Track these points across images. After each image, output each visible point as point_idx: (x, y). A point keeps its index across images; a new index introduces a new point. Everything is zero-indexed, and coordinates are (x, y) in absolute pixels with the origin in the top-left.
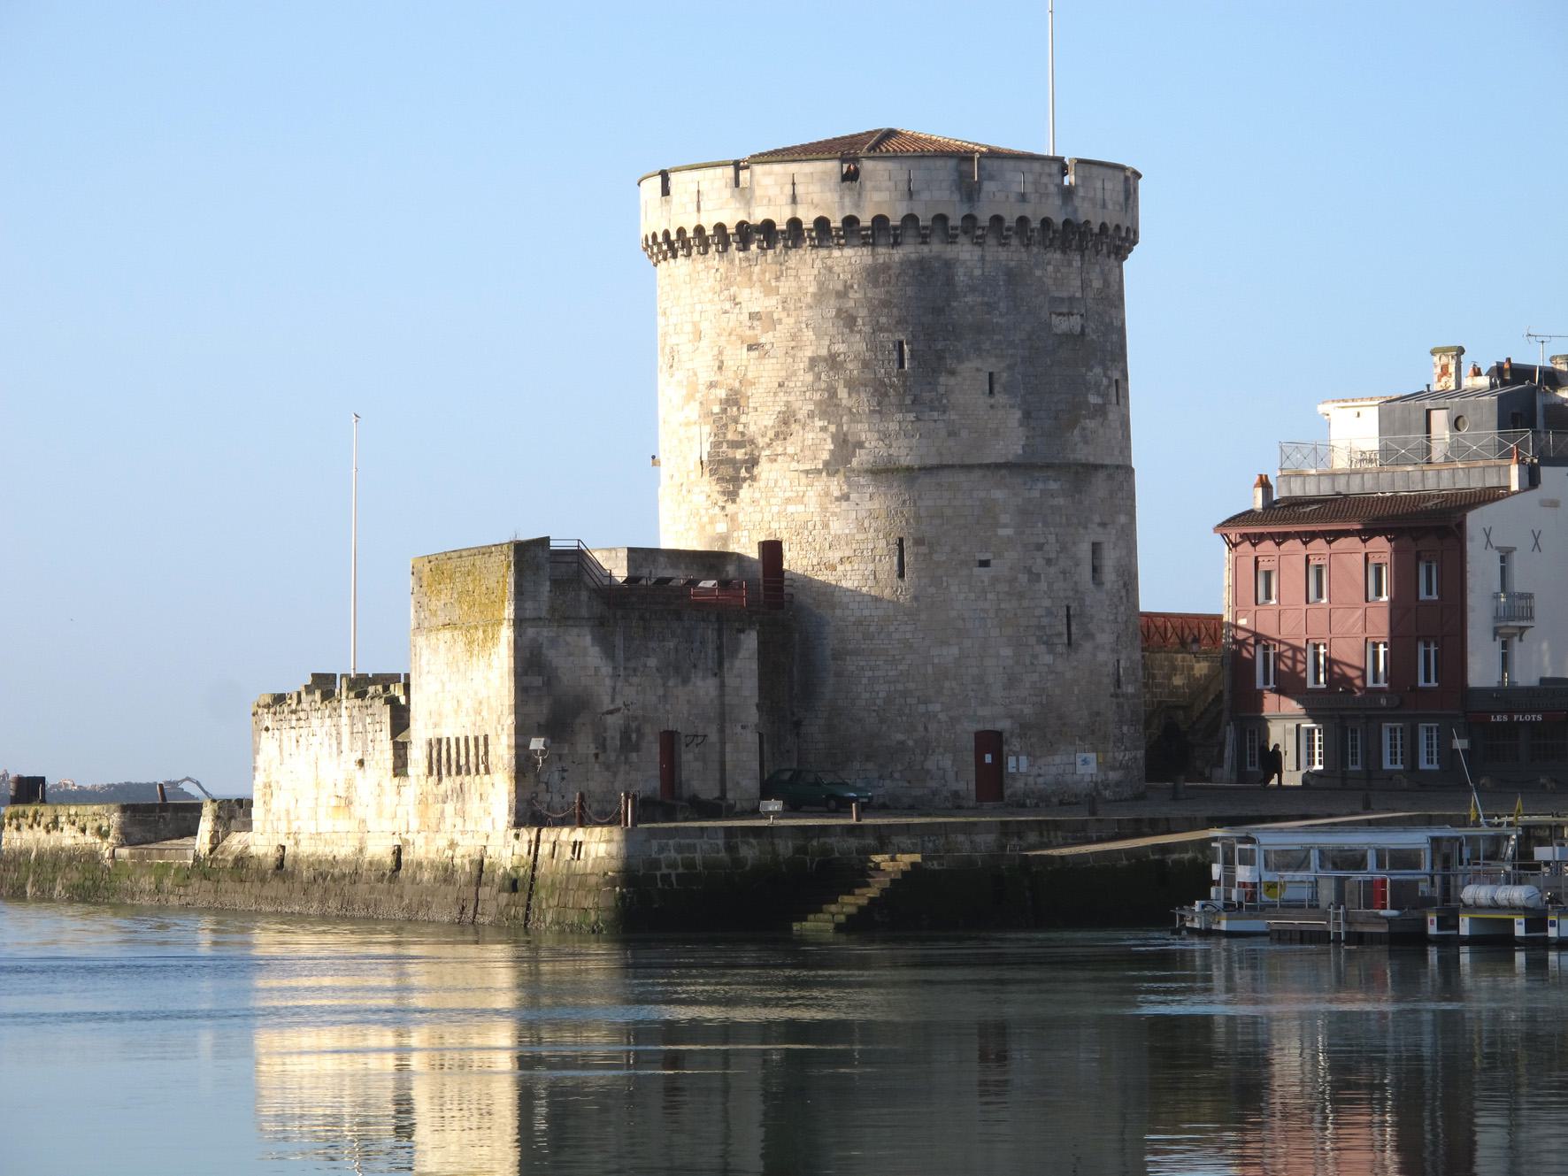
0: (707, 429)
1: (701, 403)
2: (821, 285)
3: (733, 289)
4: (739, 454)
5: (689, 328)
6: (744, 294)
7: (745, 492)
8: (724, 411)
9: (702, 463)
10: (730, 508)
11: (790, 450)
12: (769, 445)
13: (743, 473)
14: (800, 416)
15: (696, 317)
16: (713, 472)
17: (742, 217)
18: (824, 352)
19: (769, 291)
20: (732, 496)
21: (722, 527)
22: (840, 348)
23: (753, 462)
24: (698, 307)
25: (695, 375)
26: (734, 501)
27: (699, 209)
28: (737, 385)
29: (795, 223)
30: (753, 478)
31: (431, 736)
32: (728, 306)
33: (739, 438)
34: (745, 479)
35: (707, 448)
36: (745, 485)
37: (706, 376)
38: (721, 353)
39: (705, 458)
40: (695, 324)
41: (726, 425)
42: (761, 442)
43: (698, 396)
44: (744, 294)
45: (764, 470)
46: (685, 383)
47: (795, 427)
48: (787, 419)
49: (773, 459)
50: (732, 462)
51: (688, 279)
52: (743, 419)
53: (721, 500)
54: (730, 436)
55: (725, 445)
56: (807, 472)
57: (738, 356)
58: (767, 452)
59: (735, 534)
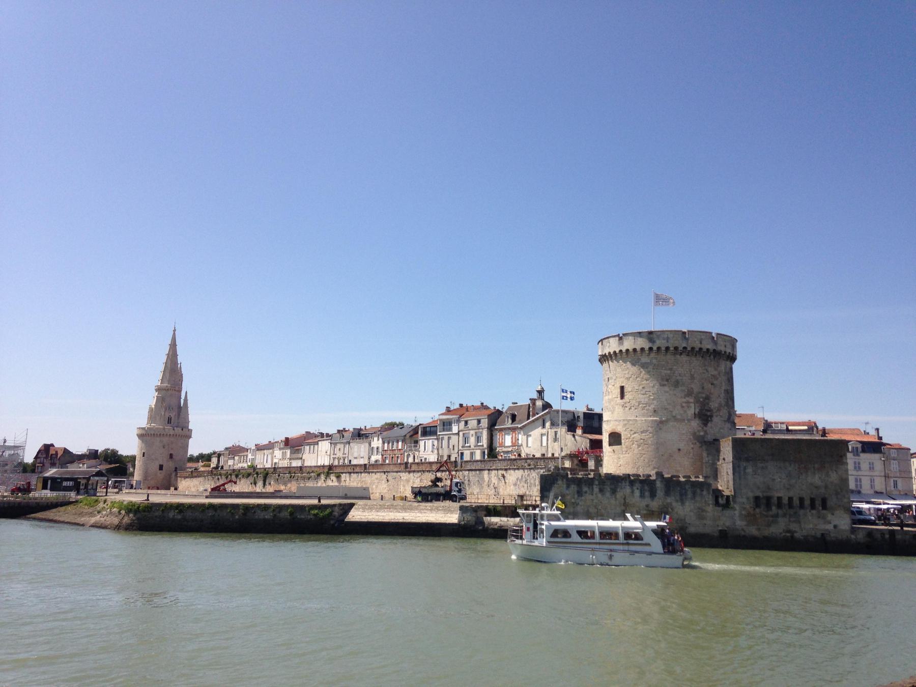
1: (695, 397)
2: (725, 370)
3: (706, 367)
4: (709, 414)
6: (709, 369)
7: (709, 425)
8: (704, 401)
9: (695, 413)
10: (705, 428)
11: (721, 414)
12: (716, 412)
13: (709, 419)
14: (723, 405)
15: (692, 373)
16: (700, 418)
17: (715, 348)
18: (726, 389)
19: (716, 369)
20: (706, 425)
21: (702, 434)
22: (728, 388)
23: (711, 416)
24: (693, 370)
26: (706, 427)
27: (701, 343)
28: (708, 394)
29: (725, 352)
30: (712, 421)
31: (760, 495)
32: (705, 371)
33: (709, 409)
34: (710, 421)
36: (710, 422)
37: (696, 390)
38: (703, 384)
39: (696, 413)
41: (705, 405)
42: (714, 411)
44: (709, 369)
45: (716, 419)
46: (686, 391)
47: (722, 408)
48: (720, 405)
49: (717, 416)
50: (706, 415)
52: (710, 404)
53: (702, 426)
54: (706, 408)
55: (704, 411)
56: (725, 421)
57: (708, 386)
58: (716, 414)
59: (706, 436)
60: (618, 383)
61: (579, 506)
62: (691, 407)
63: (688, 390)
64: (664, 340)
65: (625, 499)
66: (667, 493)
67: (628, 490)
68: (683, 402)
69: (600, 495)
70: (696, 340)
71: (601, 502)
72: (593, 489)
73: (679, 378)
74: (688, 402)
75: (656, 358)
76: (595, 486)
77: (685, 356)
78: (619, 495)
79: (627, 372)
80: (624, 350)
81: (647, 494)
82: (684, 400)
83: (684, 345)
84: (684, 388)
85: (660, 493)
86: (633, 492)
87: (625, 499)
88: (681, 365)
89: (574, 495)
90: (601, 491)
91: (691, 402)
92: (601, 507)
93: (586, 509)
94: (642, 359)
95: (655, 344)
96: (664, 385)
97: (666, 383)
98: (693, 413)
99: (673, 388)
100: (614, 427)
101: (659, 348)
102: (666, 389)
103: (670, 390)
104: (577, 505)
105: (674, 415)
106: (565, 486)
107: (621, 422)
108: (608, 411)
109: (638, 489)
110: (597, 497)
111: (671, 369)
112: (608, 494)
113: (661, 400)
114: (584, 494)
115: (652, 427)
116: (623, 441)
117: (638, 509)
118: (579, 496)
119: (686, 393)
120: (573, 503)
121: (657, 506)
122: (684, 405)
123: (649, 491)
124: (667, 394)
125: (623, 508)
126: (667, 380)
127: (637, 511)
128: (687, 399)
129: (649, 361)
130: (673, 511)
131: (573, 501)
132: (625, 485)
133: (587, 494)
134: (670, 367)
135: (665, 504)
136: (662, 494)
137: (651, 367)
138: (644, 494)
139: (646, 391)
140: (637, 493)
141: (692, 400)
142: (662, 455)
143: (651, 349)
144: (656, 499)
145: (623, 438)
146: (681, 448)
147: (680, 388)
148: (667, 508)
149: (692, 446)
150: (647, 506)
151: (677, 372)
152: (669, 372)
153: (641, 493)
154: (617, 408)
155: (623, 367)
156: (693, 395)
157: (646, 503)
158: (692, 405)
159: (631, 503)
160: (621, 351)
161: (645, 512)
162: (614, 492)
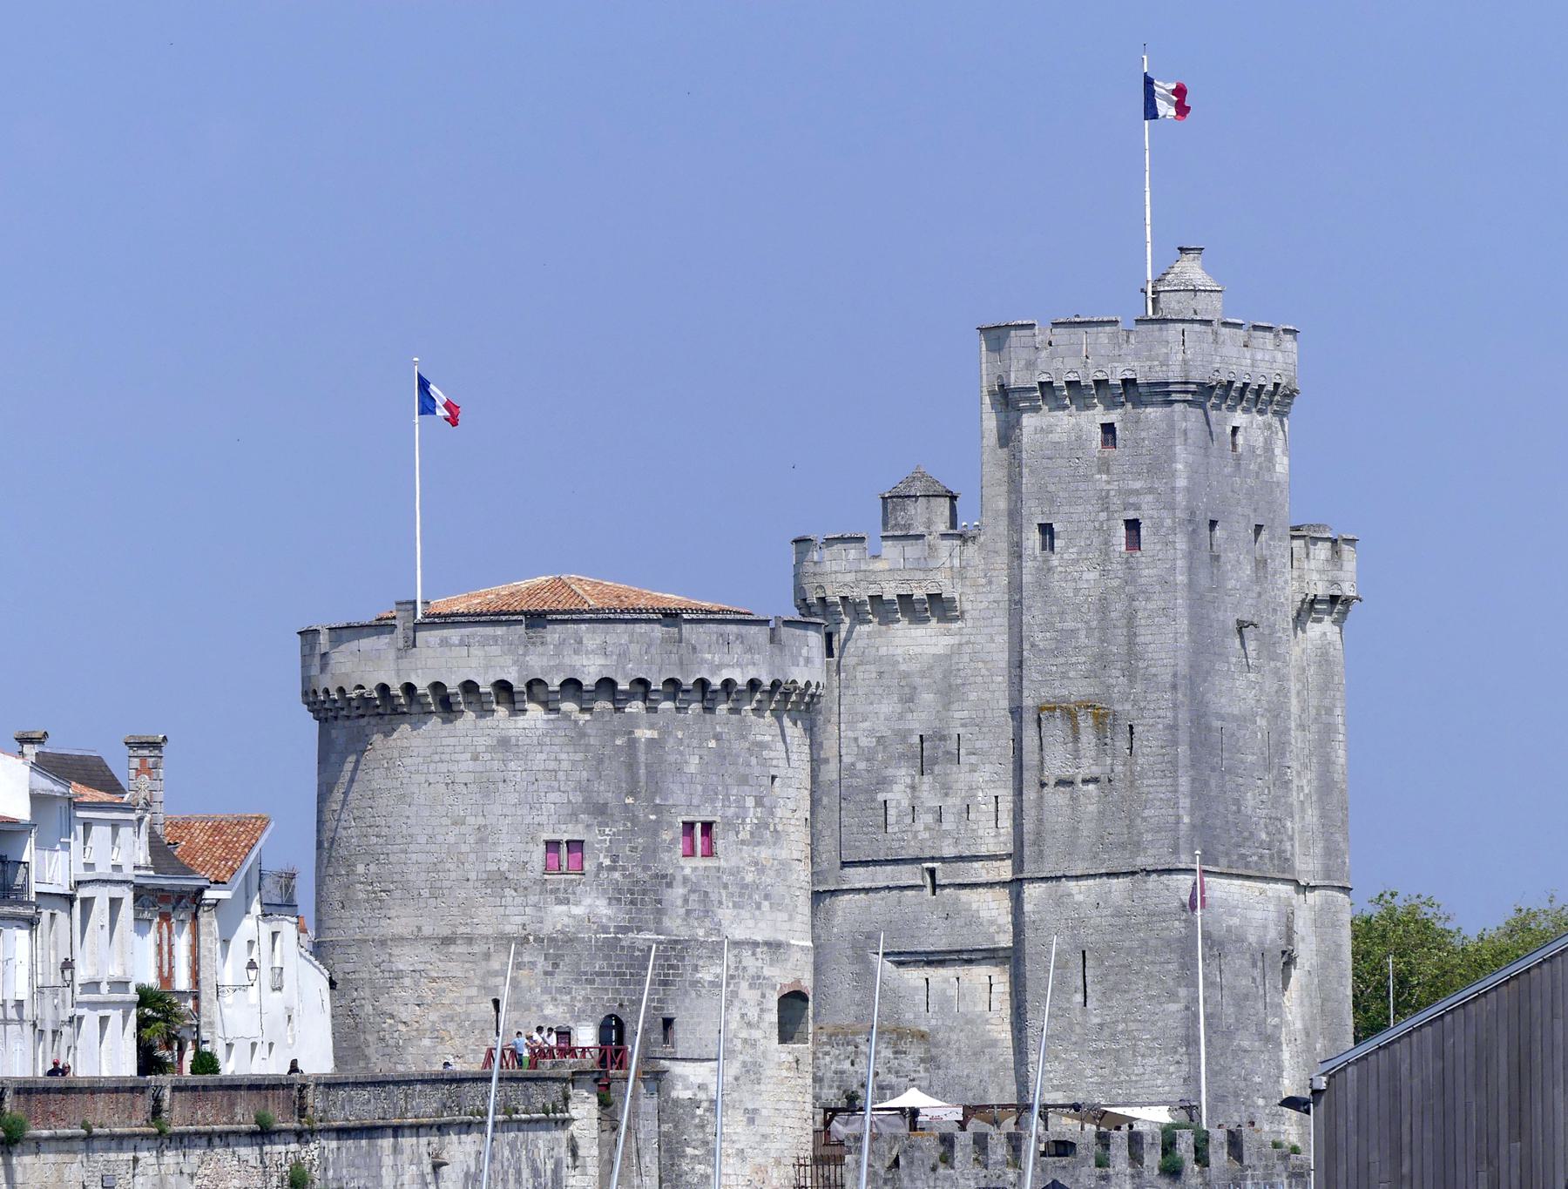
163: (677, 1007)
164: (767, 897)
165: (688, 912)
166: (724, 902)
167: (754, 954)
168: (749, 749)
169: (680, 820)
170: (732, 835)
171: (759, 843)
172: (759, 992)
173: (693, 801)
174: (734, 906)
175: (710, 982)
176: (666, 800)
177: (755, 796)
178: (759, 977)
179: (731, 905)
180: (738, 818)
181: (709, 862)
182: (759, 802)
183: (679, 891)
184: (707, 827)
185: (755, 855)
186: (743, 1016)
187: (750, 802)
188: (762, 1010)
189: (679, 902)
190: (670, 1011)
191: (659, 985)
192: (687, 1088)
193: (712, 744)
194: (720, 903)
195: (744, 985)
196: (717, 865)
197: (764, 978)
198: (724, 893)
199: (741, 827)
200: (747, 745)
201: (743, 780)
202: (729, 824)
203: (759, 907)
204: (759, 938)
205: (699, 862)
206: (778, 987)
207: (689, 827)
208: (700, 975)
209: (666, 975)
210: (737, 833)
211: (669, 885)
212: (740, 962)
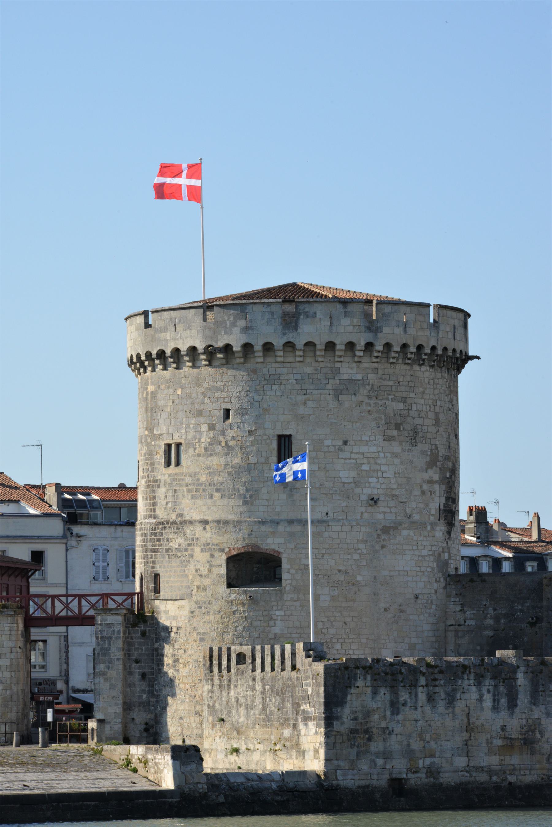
0: (443, 487)
5: (431, 415)
9: (440, 509)
15: (438, 410)
21: (446, 556)
25: (437, 448)
27: (454, 338)
35: (443, 500)
39: (442, 507)
40: (437, 414)
43: (439, 464)
46: (429, 453)
51: (431, 381)
60: (268, 425)
61: (393, 736)
62: (435, 492)
63: (431, 450)
64: (398, 326)
65: (468, 715)
66: (534, 700)
67: (473, 693)
68: (424, 481)
69: (428, 709)
70: (448, 329)
71: (430, 725)
72: (416, 695)
73: (418, 421)
74: (431, 482)
75: (376, 371)
76: (420, 689)
77: (428, 368)
78: (460, 706)
79: (300, 398)
80: (300, 342)
81: (504, 701)
82: (426, 476)
83: (433, 343)
84: (426, 447)
85: (523, 699)
86: (480, 699)
87: (468, 715)
88: (421, 389)
89: (385, 711)
90: (430, 699)
91: (436, 482)
92: (431, 738)
93: (405, 743)
94: (343, 371)
95: (380, 335)
96: (390, 439)
97: (395, 433)
98: (438, 507)
99: (407, 446)
100: (253, 540)
101: (388, 346)
102: (396, 447)
103: (403, 451)
104: (390, 733)
105: (408, 511)
106: (369, 690)
107: (281, 528)
108: (223, 496)
109: (489, 691)
110: (423, 713)
111: (404, 400)
112: (441, 706)
113: (385, 475)
114: (402, 708)
115: (365, 542)
116: (285, 576)
117: (489, 736)
118: (393, 713)
119: (428, 459)
120: (384, 730)
121: (519, 729)
122: (425, 487)
123: (507, 695)
124: (397, 461)
125: (465, 735)
126: (397, 427)
127: (487, 740)
128: (430, 472)
129: (359, 377)
130: (542, 737)
131: (383, 725)
132: (469, 685)
133: (407, 709)
134: (404, 395)
135: (530, 721)
136: (526, 701)
137: (364, 391)
138: (499, 701)
139: (352, 453)
140: (488, 702)
141: (436, 477)
142: (385, 610)
143: (369, 345)
144: (517, 710)
145: (285, 565)
146: (418, 591)
147: (420, 447)
148: (533, 731)
149: (435, 586)
150: (503, 728)
151: (414, 407)
152: (400, 406)
153: (494, 700)
154: (264, 490)
155: (289, 387)
156: (438, 464)
157: (502, 723)
158: (437, 487)
159: (478, 723)
160: (289, 345)
161: (500, 742)
162: (451, 701)
163: (160, 567)
164: (218, 490)
165: (167, 503)
166: (186, 496)
167: (204, 529)
168: (203, 393)
169: (163, 443)
170: (191, 451)
171: (211, 455)
172: (209, 554)
173: (170, 430)
174: (192, 498)
175: (176, 549)
176: (157, 431)
177: (208, 424)
178: (208, 544)
179: (190, 497)
180: (195, 440)
181: (177, 470)
182: (212, 427)
183: (163, 490)
184: (178, 445)
185: (208, 463)
186: (197, 570)
187: (204, 428)
188: (211, 566)
189: (163, 497)
190: (158, 569)
191: (153, 552)
192: (167, 619)
193: (179, 391)
194: (183, 496)
195: (197, 550)
196: (181, 471)
197: (213, 545)
198: (185, 489)
199: (197, 445)
200: (202, 390)
201: (200, 413)
202: (190, 444)
203: (211, 497)
204: (210, 518)
205: (172, 469)
206: (227, 550)
207: (169, 446)
208: (171, 544)
209: (155, 545)
210: (195, 449)
211: (159, 487)
212: (195, 534)
